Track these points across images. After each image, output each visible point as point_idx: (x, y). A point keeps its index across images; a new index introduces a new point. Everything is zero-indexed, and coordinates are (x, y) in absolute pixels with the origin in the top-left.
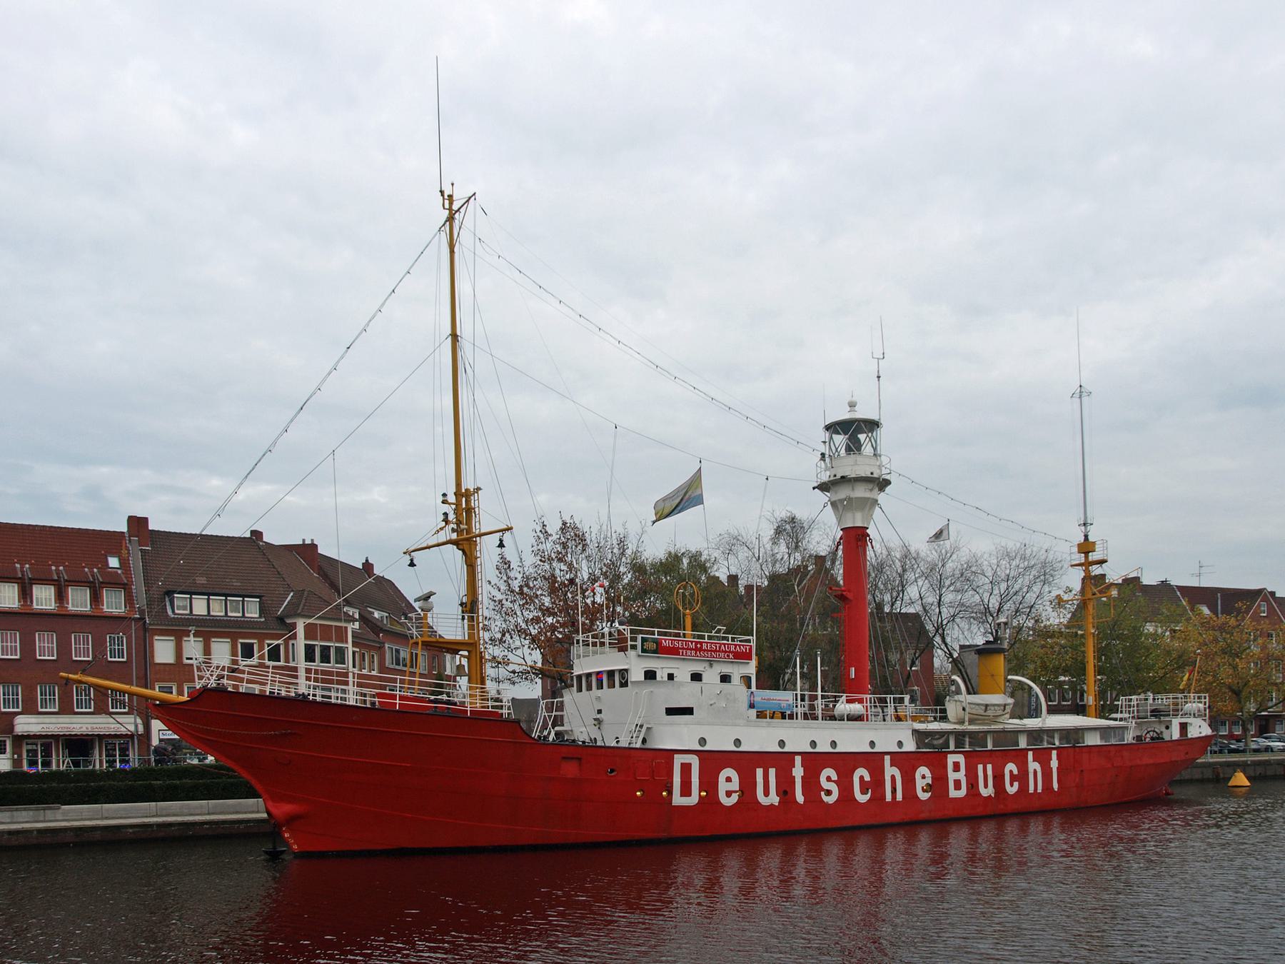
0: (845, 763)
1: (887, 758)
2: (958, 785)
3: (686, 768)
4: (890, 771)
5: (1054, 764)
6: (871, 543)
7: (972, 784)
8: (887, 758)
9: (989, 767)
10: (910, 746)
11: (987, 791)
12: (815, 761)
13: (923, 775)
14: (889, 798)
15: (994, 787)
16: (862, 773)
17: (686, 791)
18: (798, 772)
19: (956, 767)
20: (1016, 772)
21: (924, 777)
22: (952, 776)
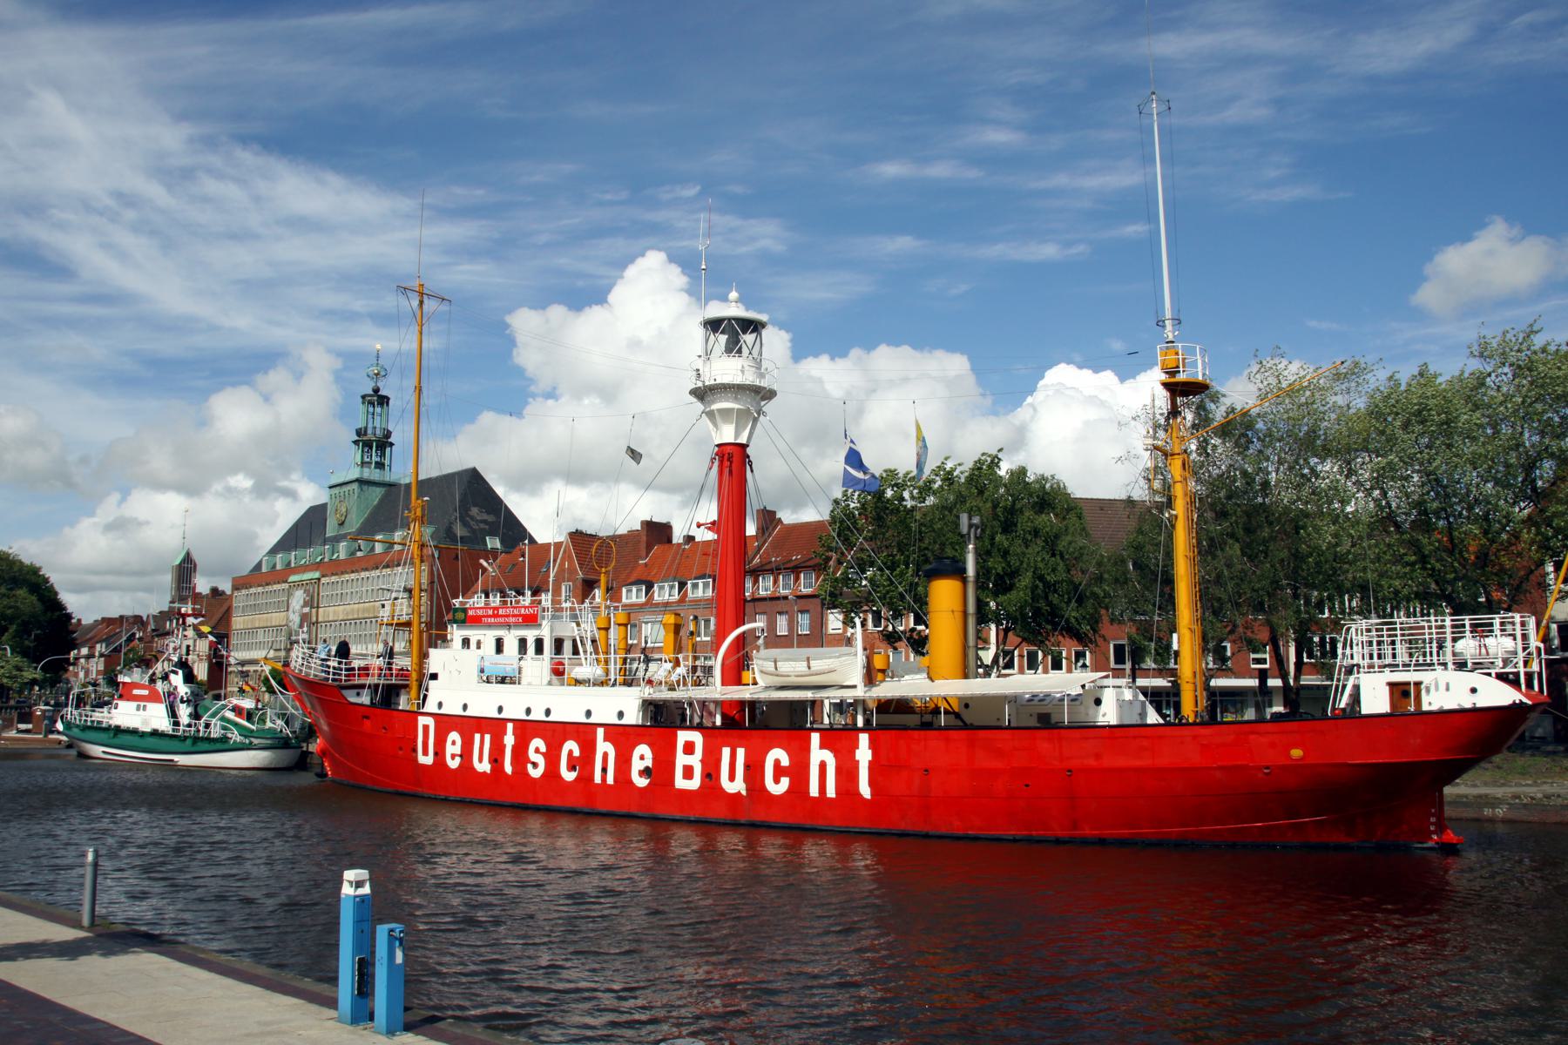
0: (555, 732)
1: (600, 732)
2: (688, 772)
3: (426, 728)
4: (604, 747)
5: (864, 754)
6: (751, 466)
7: (711, 773)
8: (600, 732)
9: (741, 752)
10: (633, 717)
11: (735, 786)
12: (526, 729)
13: (643, 756)
14: (598, 779)
15: (745, 780)
16: (571, 746)
17: (425, 753)
18: (509, 740)
19: (689, 748)
20: (785, 762)
21: (642, 758)
22: (681, 760)
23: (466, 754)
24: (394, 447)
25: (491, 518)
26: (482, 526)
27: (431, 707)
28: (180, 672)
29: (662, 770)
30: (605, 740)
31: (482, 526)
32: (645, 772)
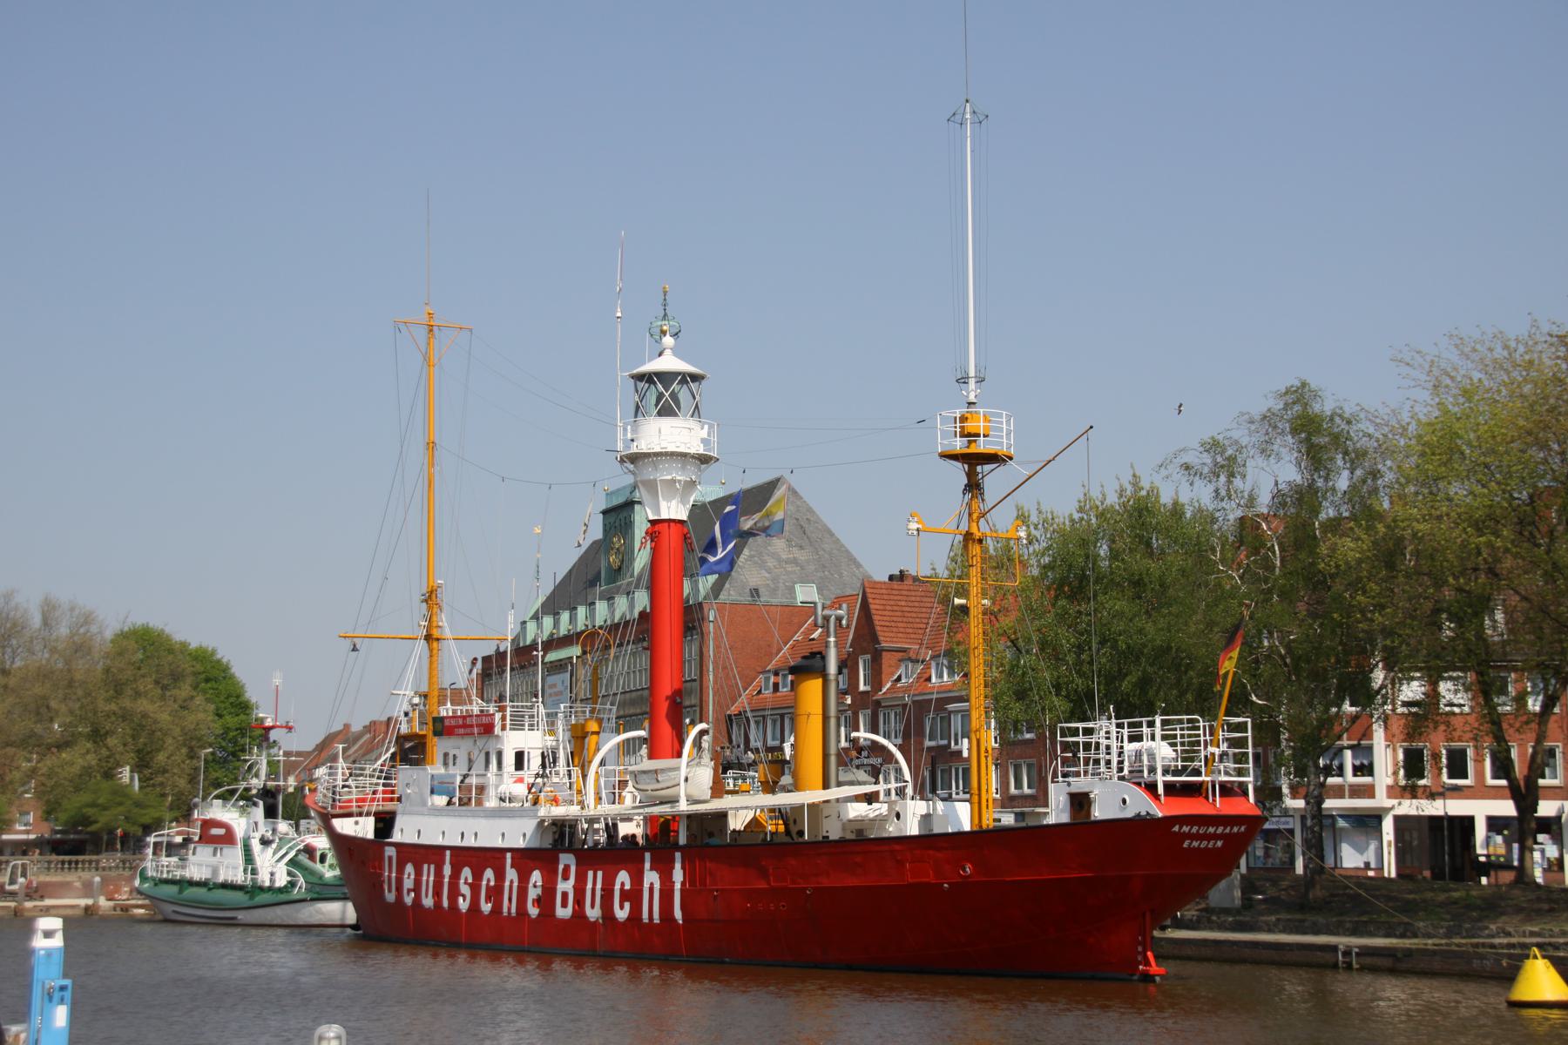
4: (511, 875)
5: (678, 875)
7: (579, 901)
9: (600, 874)
16: (489, 874)
18: (447, 870)
23: (417, 888)
27: (397, 837)
28: (261, 803)
29: (546, 900)
30: (512, 867)
31: (789, 568)
32: (538, 901)
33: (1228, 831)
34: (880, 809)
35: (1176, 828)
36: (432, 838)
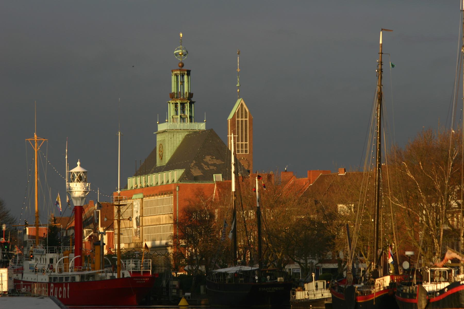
24: (195, 103)
25: (218, 162)
26: (212, 167)
31: (212, 167)
33: (145, 279)
34: (104, 274)
35: (134, 279)
36: (29, 280)
